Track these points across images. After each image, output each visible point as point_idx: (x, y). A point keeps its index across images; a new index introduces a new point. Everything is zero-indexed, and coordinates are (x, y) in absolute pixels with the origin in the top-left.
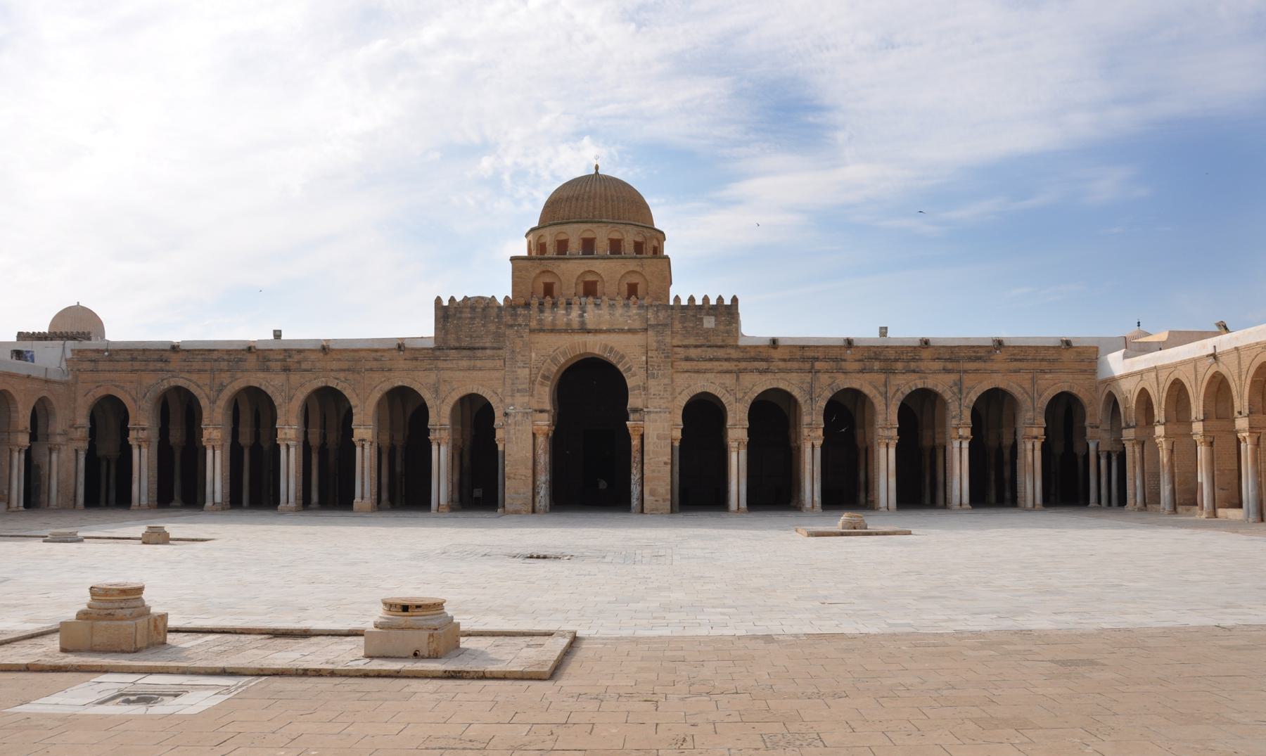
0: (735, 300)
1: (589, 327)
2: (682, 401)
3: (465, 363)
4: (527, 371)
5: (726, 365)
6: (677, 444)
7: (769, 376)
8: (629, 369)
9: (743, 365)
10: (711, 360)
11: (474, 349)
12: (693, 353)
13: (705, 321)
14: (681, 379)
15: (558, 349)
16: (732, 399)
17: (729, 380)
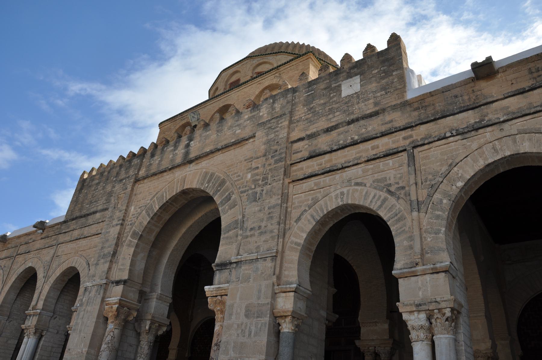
0: (395, 41)
1: (192, 156)
2: (301, 231)
3: (76, 234)
4: (118, 227)
5: (385, 144)
6: (287, 327)
7: (488, 134)
8: (228, 198)
9: (422, 131)
10: (354, 143)
11: (88, 215)
12: (323, 142)
13: (343, 88)
14: (300, 194)
15: (154, 193)
16: (401, 206)
17: (393, 169)
